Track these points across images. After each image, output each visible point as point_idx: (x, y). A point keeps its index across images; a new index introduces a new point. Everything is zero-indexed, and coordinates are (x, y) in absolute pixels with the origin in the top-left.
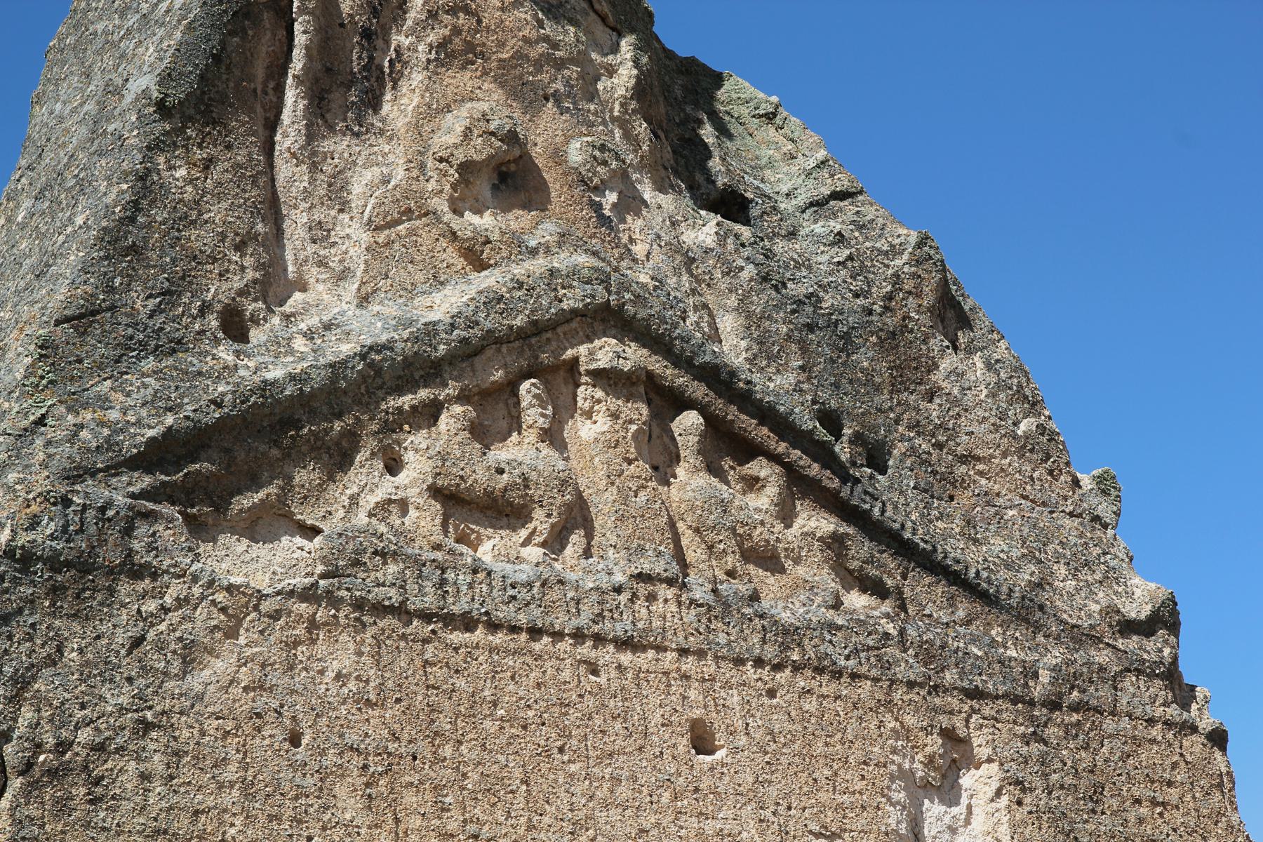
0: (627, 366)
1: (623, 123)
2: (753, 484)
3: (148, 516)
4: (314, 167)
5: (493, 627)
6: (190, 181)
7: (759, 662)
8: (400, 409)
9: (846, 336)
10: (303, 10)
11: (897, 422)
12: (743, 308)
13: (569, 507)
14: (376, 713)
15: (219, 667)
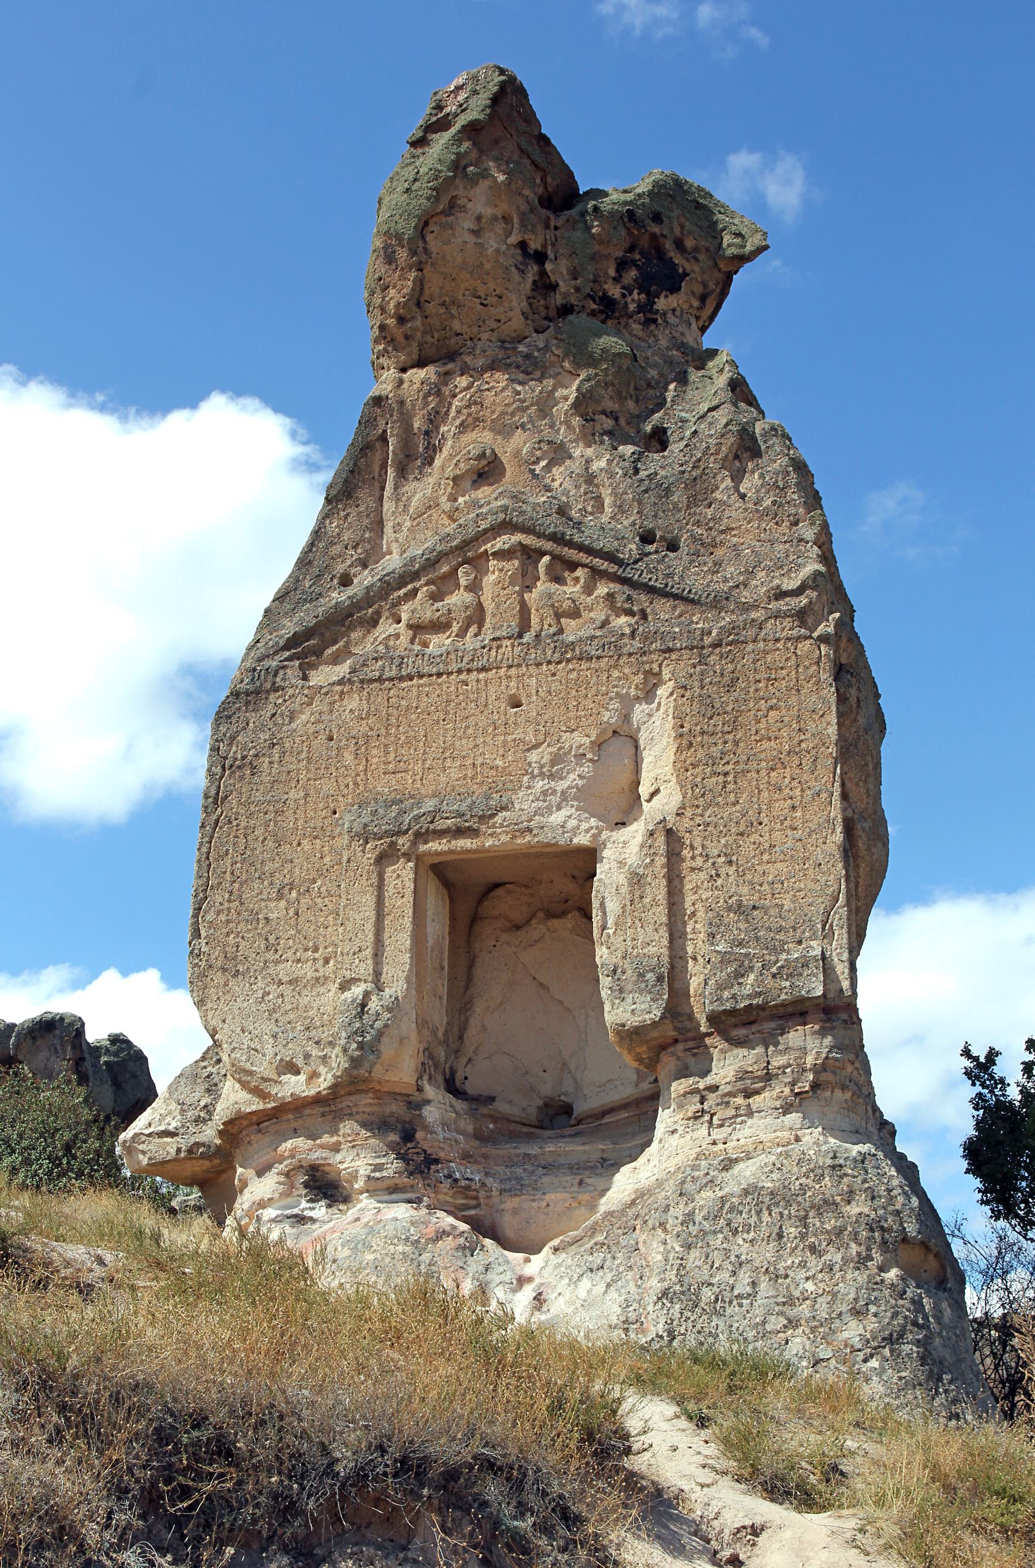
0: (507, 546)
1: (567, 423)
2: (577, 580)
3: (284, 667)
4: (398, 500)
5: (421, 676)
6: (338, 526)
7: (549, 663)
8: (399, 597)
9: (668, 489)
10: (392, 435)
11: (687, 524)
12: (614, 494)
13: (469, 617)
15: (304, 717)
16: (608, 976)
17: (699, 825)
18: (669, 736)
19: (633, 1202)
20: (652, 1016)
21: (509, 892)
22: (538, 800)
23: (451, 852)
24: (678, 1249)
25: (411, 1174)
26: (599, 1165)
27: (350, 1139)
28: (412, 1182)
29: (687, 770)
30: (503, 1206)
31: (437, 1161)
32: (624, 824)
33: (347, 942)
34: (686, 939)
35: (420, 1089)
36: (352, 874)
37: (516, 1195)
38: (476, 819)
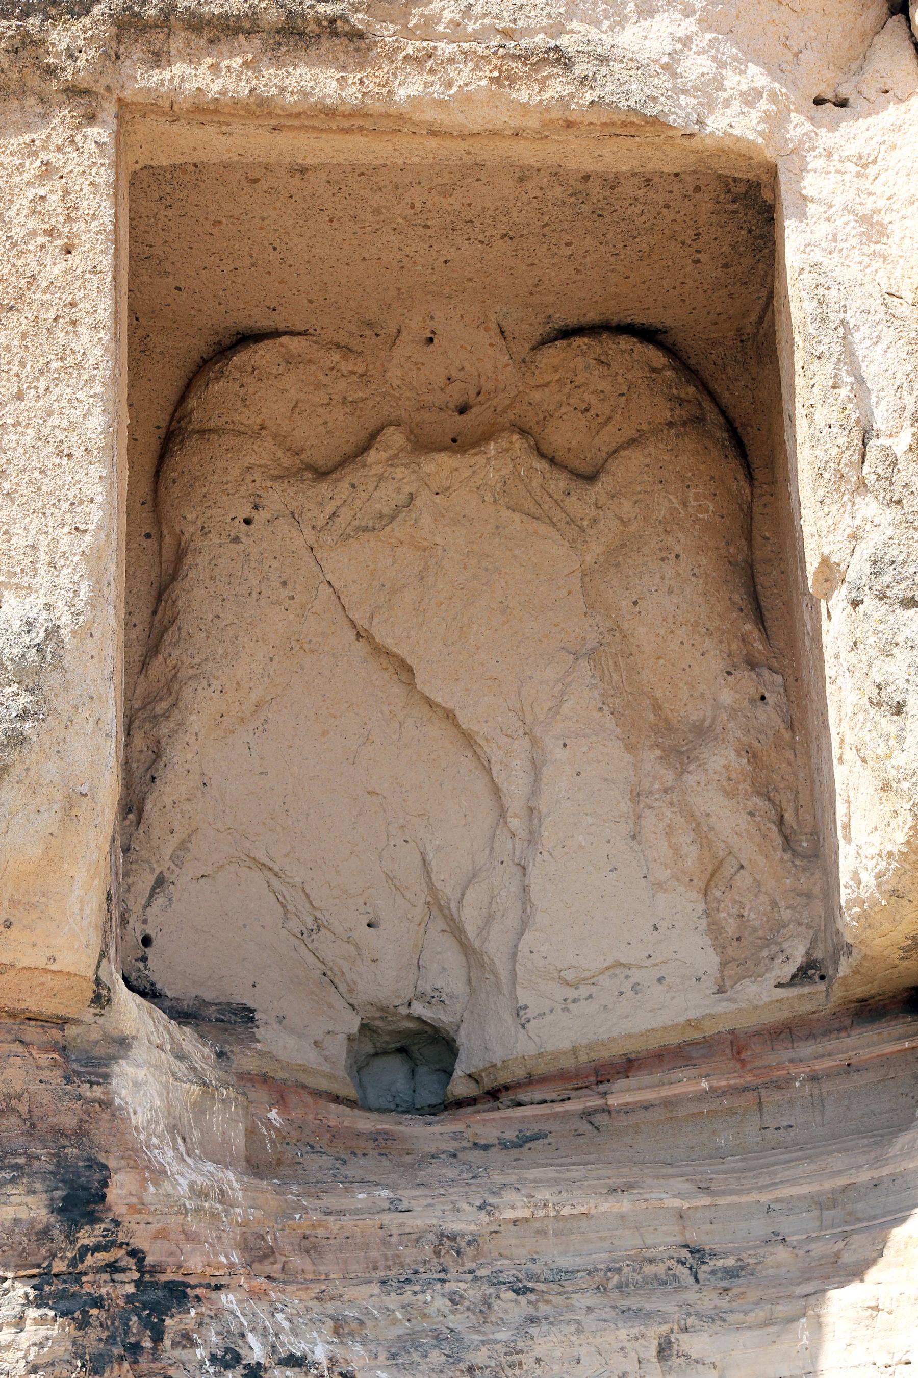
21: (290, 360)
26: (683, 1272)
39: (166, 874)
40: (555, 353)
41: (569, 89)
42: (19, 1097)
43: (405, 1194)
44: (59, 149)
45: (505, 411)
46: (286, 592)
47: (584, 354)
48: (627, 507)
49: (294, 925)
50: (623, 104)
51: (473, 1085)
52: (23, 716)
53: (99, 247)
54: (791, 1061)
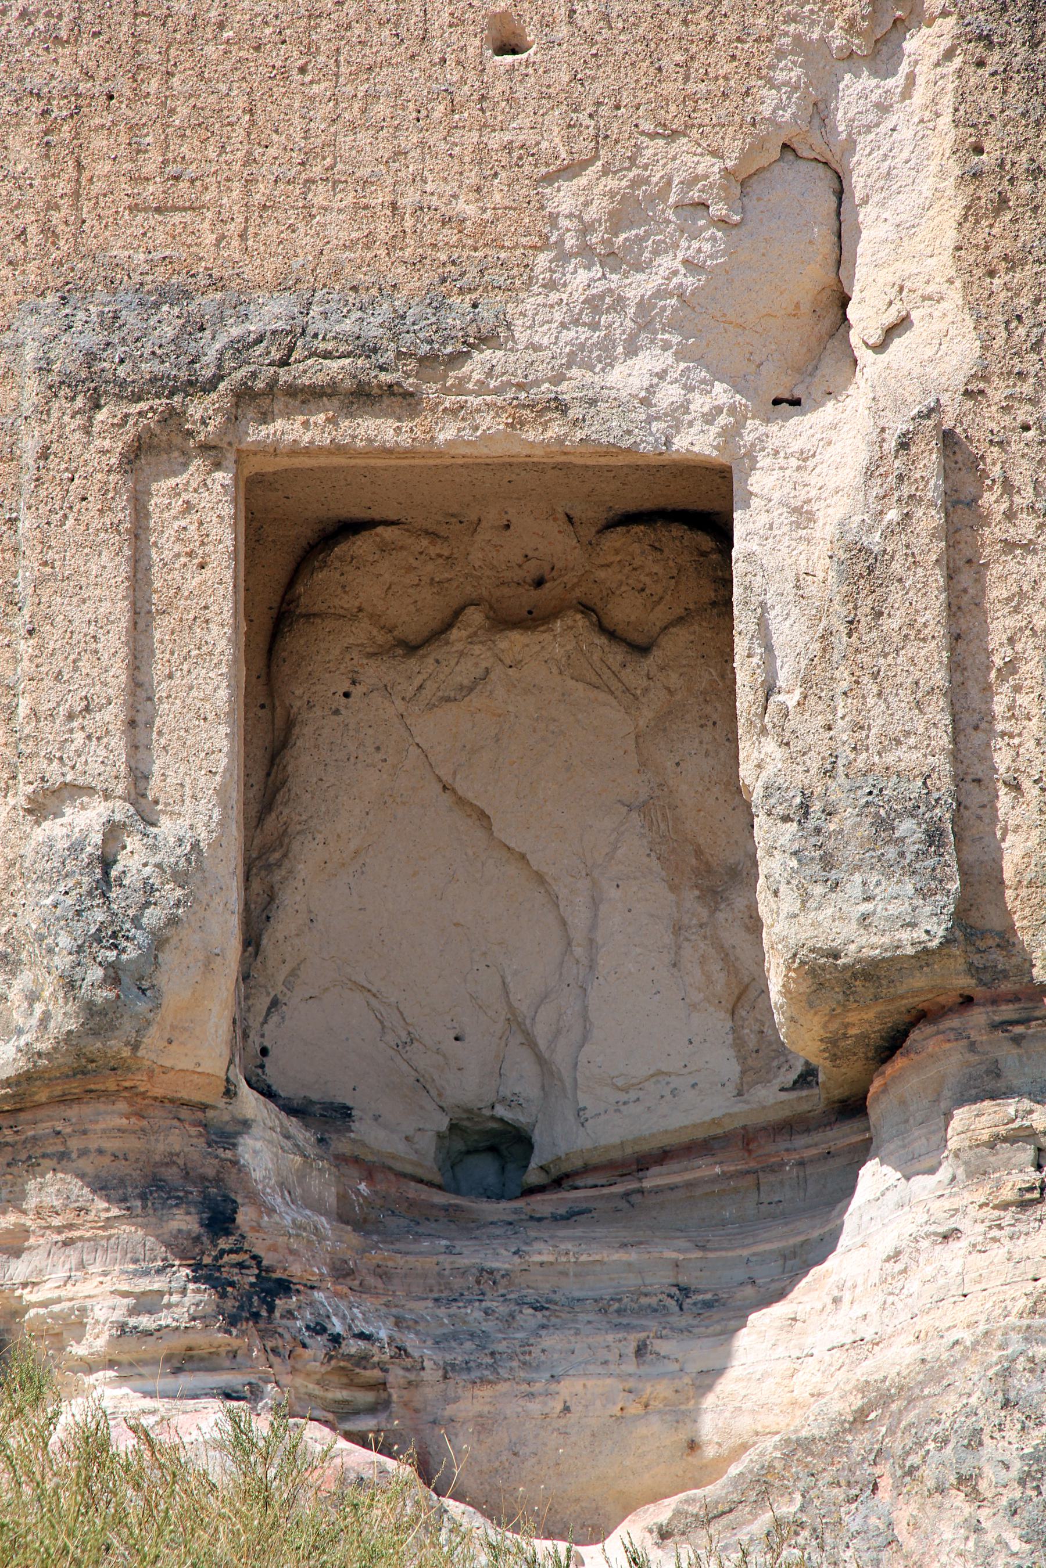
14: (67, 51)
16: (786, 819)
17: (1026, 428)
18: (942, 174)
19: (860, 1418)
20: (919, 934)
21: (385, 548)
22: (576, 322)
23: (337, 449)
24: (1016, 1545)
25: (233, 1321)
26: (672, 1304)
27: (56, 1222)
28: (236, 1343)
29: (992, 274)
30: (450, 1410)
31: (284, 1287)
32: (796, 402)
33: (48, 682)
34: (991, 732)
35: (230, 1092)
36: (57, 492)
37: (484, 1381)
38: (412, 365)
39: (279, 996)
40: (616, 538)
41: (566, 429)
42: (178, 1155)
43: (457, 1243)
44: (196, 490)
45: (573, 588)
46: (380, 756)
47: (640, 541)
48: (674, 679)
49: (390, 1038)
50: (604, 440)
51: (543, 1175)
52: (177, 905)
53: (224, 564)
54: (787, 1150)
